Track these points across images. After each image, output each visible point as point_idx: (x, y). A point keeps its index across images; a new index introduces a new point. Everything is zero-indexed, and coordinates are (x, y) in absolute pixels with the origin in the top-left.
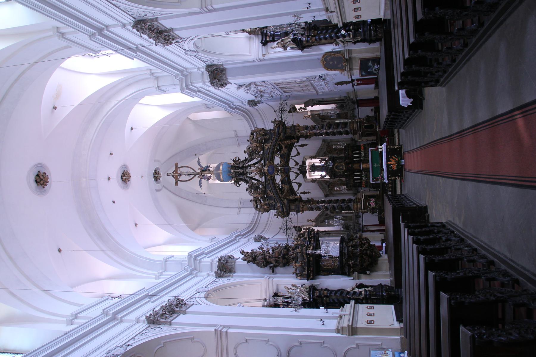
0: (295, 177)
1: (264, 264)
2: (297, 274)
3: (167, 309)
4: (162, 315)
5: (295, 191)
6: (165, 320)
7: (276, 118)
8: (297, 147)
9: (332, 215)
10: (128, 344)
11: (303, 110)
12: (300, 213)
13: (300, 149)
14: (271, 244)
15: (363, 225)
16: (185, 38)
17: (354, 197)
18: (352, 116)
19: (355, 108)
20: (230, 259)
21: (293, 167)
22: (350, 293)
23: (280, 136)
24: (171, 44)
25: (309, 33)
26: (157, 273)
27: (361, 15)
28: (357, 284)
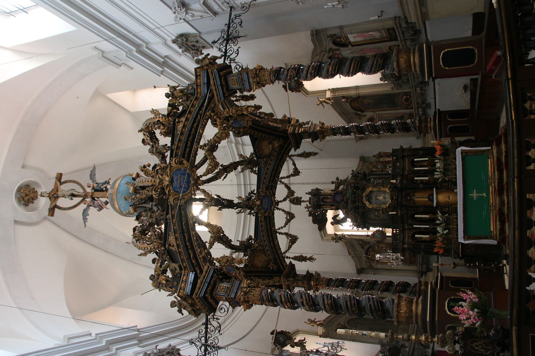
0: (284, 221)
13: (301, 163)
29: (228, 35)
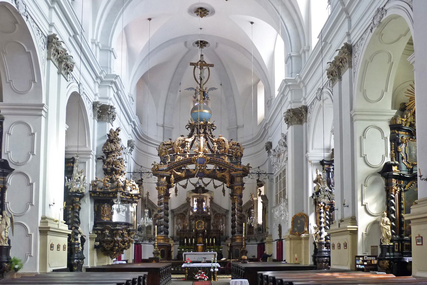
1: (106, 150)
2: (96, 181)
3: (63, 56)
4: (57, 51)
5: (179, 182)
6: (53, 54)
7: (251, 168)
8: (222, 186)
9: (153, 216)
10: (29, 17)
11: (258, 193)
12: (157, 186)
13: (221, 188)
14: (126, 157)
15: (142, 244)
16: (332, 90)
17: (170, 237)
18: (250, 238)
19: (257, 241)
20: (111, 117)
21: (203, 181)
22: (76, 230)
23: (234, 171)
24: (328, 77)
25: (328, 204)
26: (98, 41)
27: (334, 249)
28: (85, 236)
29: (260, 174)
